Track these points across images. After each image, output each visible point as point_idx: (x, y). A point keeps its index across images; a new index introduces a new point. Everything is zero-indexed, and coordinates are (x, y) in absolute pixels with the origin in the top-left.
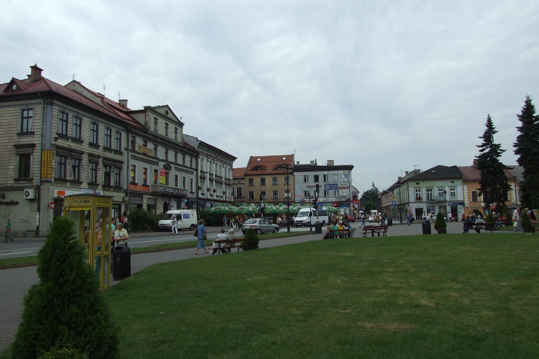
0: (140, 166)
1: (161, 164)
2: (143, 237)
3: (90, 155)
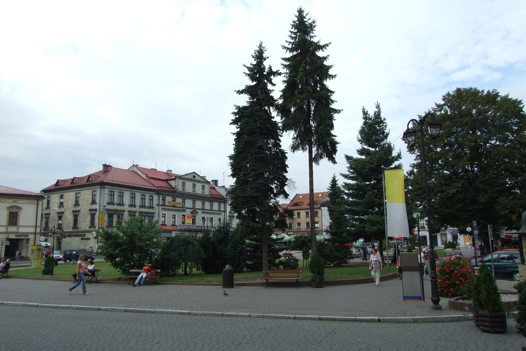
0: (169, 214)
1: (188, 212)
3: (129, 211)
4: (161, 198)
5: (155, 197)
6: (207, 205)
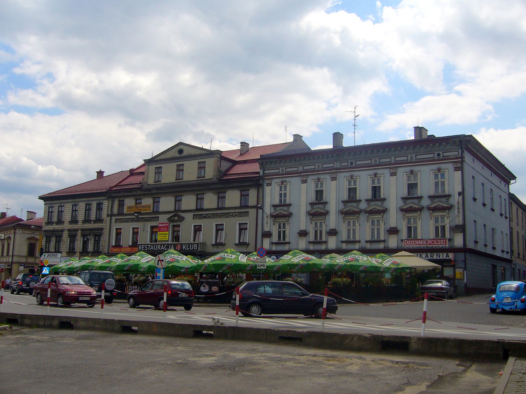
2: (209, 306)
3: (69, 230)
4: (110, 202)
5: (106, 204)
6: (210, 200)
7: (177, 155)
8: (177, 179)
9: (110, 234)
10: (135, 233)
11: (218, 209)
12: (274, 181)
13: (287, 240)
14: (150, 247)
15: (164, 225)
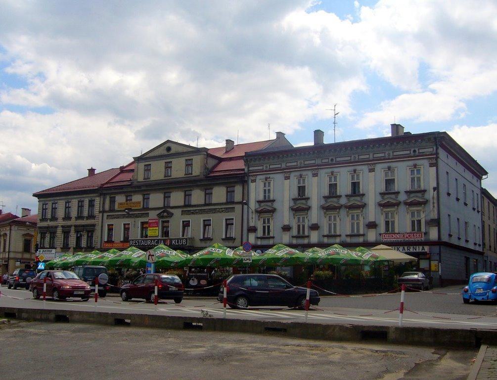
2: (198, 299)
3: (62, 227)
4: (102, 200)
5: (98, 201)
6: (197, 197)
7: (165, 153)
8: (165, 176)
9: (102, 230)
10: (126, 229)
11: (206, 205)
12: (259, 177)
13: (271, 235)
14: (141, 242)
15: (154, 221)
